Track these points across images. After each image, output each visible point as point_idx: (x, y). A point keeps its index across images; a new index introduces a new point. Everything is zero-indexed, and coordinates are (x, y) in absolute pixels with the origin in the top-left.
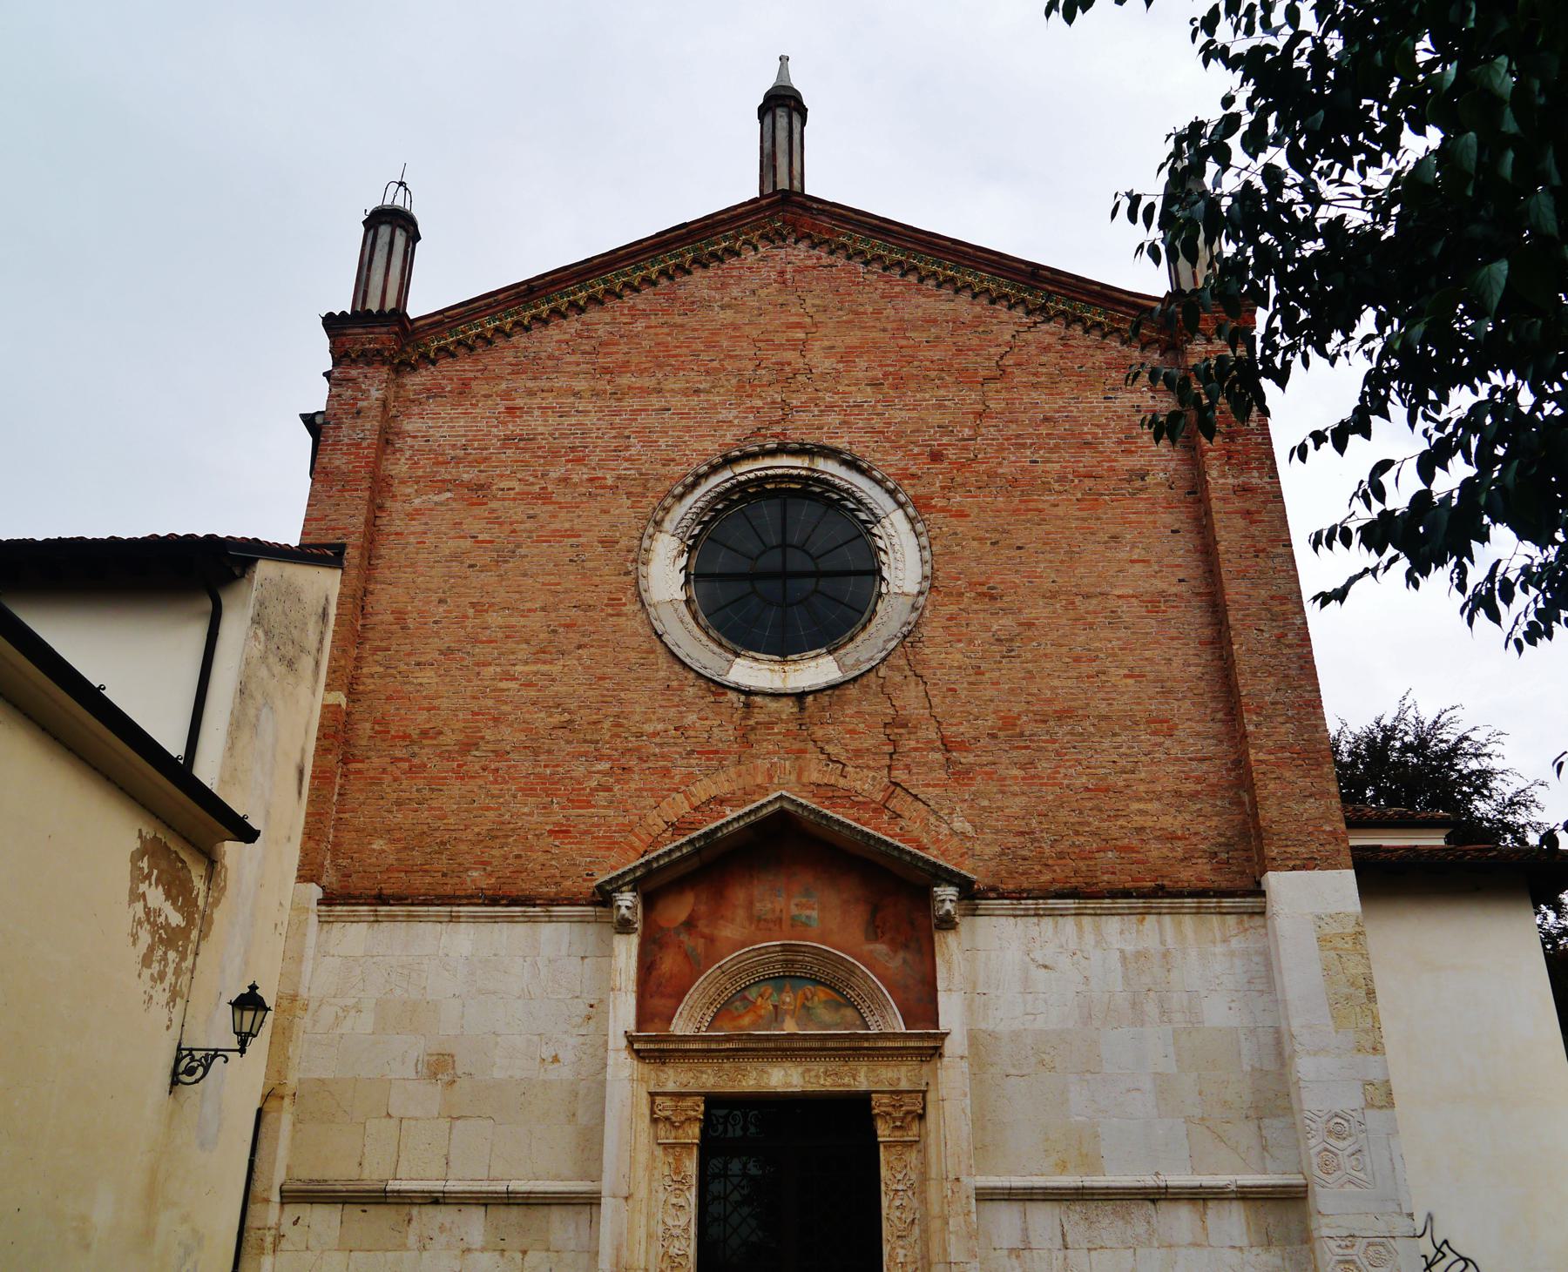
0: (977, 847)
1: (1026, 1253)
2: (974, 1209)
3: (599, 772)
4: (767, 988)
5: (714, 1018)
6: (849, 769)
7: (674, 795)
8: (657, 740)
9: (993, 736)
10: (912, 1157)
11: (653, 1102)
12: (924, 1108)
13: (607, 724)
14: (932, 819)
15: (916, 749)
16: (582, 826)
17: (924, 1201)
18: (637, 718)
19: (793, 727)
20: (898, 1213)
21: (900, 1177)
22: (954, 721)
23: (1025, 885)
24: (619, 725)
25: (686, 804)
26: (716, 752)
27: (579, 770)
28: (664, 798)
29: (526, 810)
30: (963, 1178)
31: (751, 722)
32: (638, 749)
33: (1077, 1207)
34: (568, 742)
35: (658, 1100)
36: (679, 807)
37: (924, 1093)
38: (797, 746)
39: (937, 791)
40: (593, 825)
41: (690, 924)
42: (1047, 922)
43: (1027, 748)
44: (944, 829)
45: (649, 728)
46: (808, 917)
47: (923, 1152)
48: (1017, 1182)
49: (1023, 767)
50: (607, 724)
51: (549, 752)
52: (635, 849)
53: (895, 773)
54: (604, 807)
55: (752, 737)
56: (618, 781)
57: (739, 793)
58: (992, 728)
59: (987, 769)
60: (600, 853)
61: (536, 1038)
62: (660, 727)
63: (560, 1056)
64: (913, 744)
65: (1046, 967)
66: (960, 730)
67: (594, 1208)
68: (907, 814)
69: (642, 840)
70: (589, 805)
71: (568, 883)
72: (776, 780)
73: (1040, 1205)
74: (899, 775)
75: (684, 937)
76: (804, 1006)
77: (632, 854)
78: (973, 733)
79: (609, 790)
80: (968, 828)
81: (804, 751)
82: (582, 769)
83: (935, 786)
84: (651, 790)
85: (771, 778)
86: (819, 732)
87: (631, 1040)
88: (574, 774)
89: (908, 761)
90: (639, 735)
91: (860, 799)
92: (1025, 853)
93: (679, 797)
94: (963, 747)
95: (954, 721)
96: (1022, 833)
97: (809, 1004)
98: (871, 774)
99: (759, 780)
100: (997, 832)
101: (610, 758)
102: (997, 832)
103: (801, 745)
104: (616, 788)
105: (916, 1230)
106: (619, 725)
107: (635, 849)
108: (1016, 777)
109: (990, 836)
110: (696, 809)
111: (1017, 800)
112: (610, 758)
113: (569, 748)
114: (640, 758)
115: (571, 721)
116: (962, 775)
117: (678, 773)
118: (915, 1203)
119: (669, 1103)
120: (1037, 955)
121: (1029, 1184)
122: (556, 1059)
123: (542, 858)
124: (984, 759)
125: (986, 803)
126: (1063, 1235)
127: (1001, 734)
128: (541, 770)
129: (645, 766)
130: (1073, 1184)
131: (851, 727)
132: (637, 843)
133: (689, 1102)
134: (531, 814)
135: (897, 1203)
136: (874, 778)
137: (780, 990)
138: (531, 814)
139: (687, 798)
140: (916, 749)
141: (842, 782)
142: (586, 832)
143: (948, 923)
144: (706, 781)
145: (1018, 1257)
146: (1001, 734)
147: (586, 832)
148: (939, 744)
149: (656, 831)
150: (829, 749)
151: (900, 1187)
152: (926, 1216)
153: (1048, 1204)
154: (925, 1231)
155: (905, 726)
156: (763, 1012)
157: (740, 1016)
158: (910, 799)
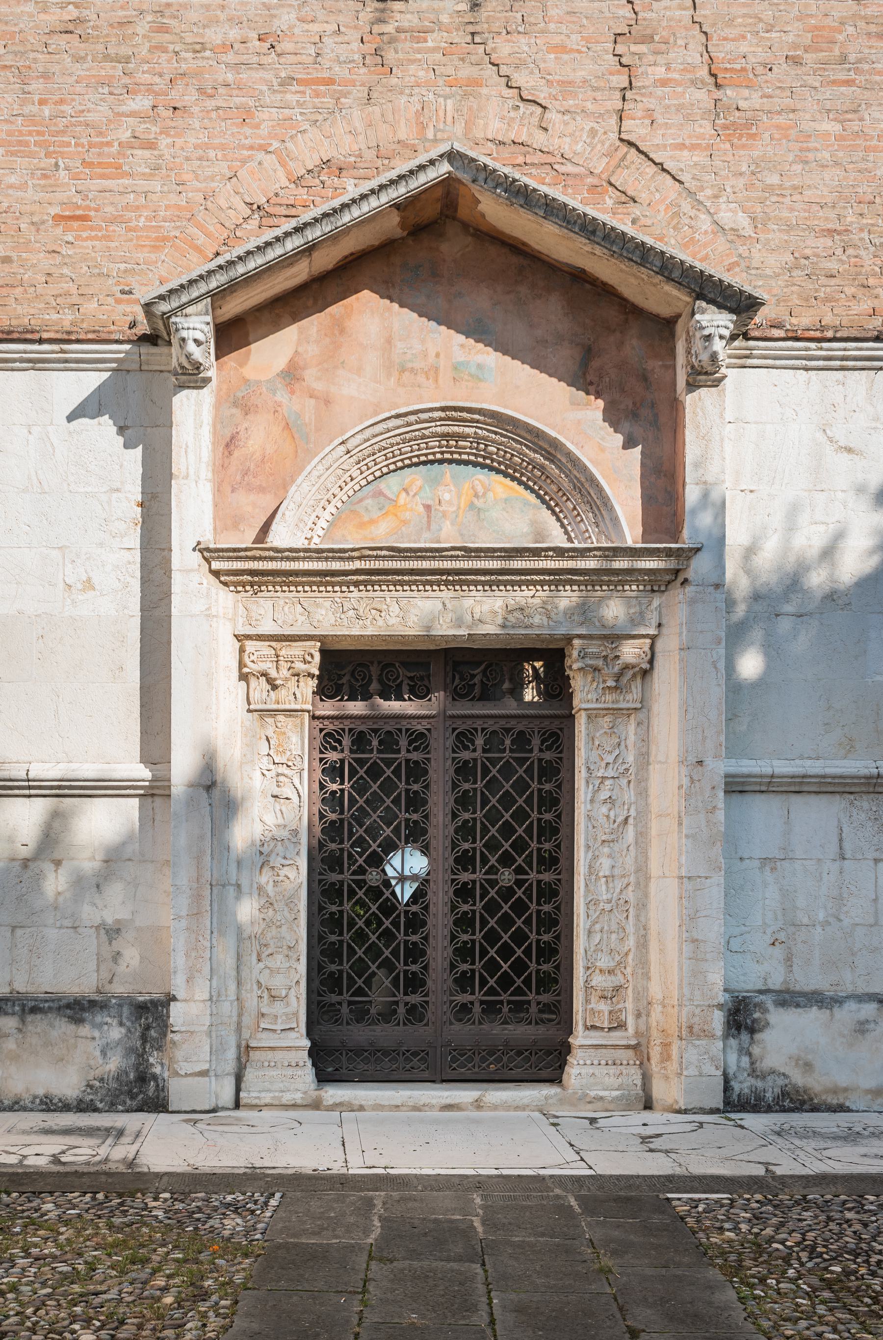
0: (756, 254)
1: (786, 864)
2: (721, 805)
3: (132, 114)
4: (415, 477)
5: (332, 524)
6: (552, 116)
7: (261, 156)
8: (230, 57)
9: (796, 61)
10: (630, 730)
11: (242, 650)
12: (651, 662)
13: (142, 27)
14: (686, 206)
15: (664, 83)
16: (109, 209)
17: (643, 793)
18: (193, 16)
19: (461, 38)
20: (604, 809)
21: (610, 758)
22: (731, 32)
23: (828, 320)
24: (163, 29)
25: (281, 174)
26: (330, 81)
27: (99, 114)
28: (244, 162)
29: (12, 179)
30: (709, 761)
31: (389, 28)
32: (198, 73)
33: (865, 803)
34: (78, 59)
35: (250, 646)
36: (267, 179)
37: (653, 638)
38: (466, 72)
39: (700, 157)
40: (127, 207)
41: (292, 374)
42: (858, 380)
43: (849, 83)
44: (705, 223)
45: (214, 36)
46: (479, 366)
47: (645, 725)
48: (783, 767)
49: (840, 116)
50: (142, 27)
51: (46, 76)
52: (198, 249)
53: (627, 124)
54: (145, 177)
55: (390, 56)
56: (165, 132)
57: (370, 155)
58: (795, 46)
59: (781, 120)
60: (141, 256)
61: (55, 553)
62: (234, 34)
63: (95, 581)
64: (660, 72)
65: (849, 450)
66: (738, 48)
67: (158, 801)
68: (643, 197)
69: (208, 235)
70: (118, 171)
71: (90, 307)
72: (430, 134)
73: (813, 799)
74: (635, 129)
75: (282, 396)
76: (471, 506)
77: (194, 257)
78: (762, 55)
79: (151, 145)
80: (743, 221)
81: (476, 83)
82: (104, 108)
83: (693, 147)
84: (223, 147)
85: (423, 127)
86: (503, 49)
87: (207, 553)
88: (91, 117)
89: (651, 103)
90: (199, 48)
91: (569, 168)
92: (832, 265)
93: (270, 160)
94: (745, 78)
95: (731, 32)
96: (831, 232)
97: (479, 503)
98: (588, 125)
99: (402, 135)
100: (790, 228)
101: (150, 89)
102: (790, 228)
103: (473, 72)
104: (164, 142)
105: (630, 832)
106: (163, 29)
107: (198, 249)
108: (827, 134)
109: (776, 236)
110: (298, 181)
111: (827, 175)
112: (150, 89)
113: (79, 70)
114: (201, 91)
115: (79, 21)
116: (735, 128)
117: (267, 117)
118: (629, 795)
119: (264, 648)
120: (838, 432)
121: (800, 771)
122: (89, 585)
123: (46, 262)
124: (778, 102)
125: (773, 179)
126: (841, 840)
127: (809, 57)
128: (35, 109)
129: (211, 104)
130: (864, 772)
131: (557, 40)
132: (201, 240)
133: (296, 650)
134: (23, 187)
135: (604, 795)
136: (593, 132)
137: (435, 482)
138: (23, 187)
139: (283, 164)
140: (664, 83)
141: (539, 139)
142: (113, 220)
143: (705, 375)
144: (313, 133)
145: (773, 869)
146: (809, 57)
147: (113, 220)
148: (704, 73)
149: (234, 218)
150: (519, 79)
151: (610, 773)
152: (643, 814)
153: (824, 798)
154: (642, 836)
155: (648, 39)
156: (407, 515)
157: (372, 522)
158: (652, 169)
